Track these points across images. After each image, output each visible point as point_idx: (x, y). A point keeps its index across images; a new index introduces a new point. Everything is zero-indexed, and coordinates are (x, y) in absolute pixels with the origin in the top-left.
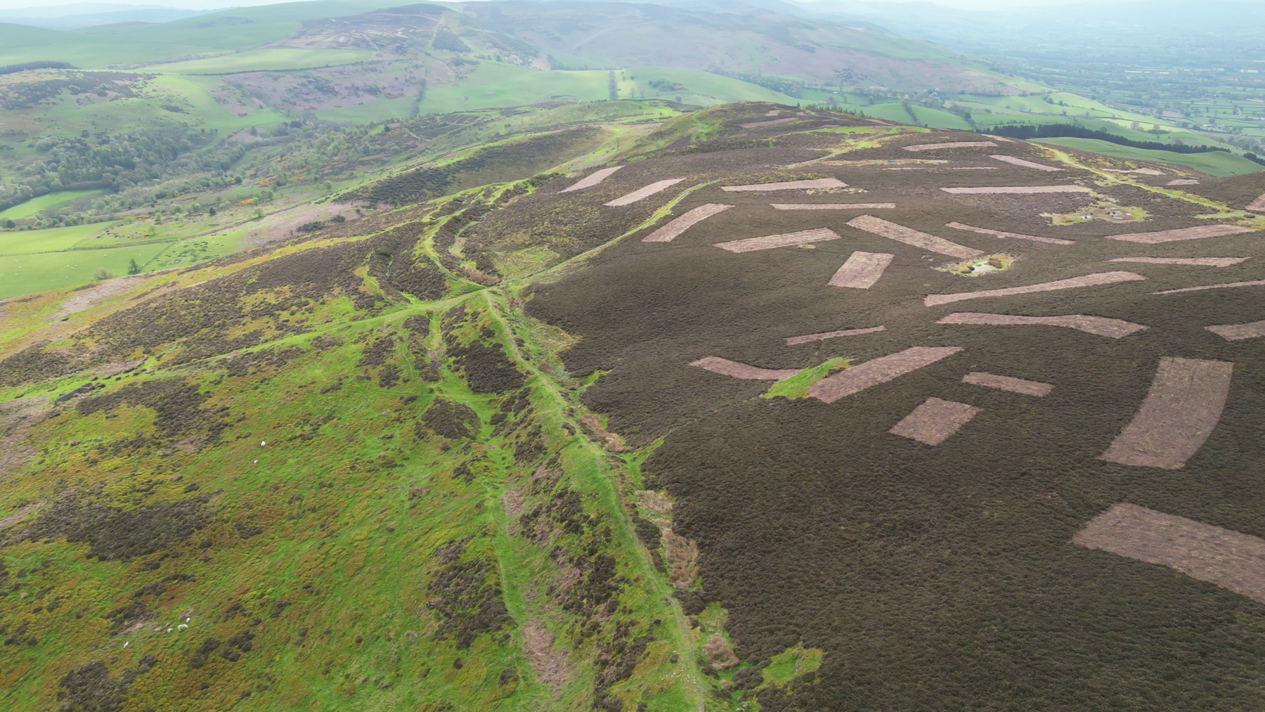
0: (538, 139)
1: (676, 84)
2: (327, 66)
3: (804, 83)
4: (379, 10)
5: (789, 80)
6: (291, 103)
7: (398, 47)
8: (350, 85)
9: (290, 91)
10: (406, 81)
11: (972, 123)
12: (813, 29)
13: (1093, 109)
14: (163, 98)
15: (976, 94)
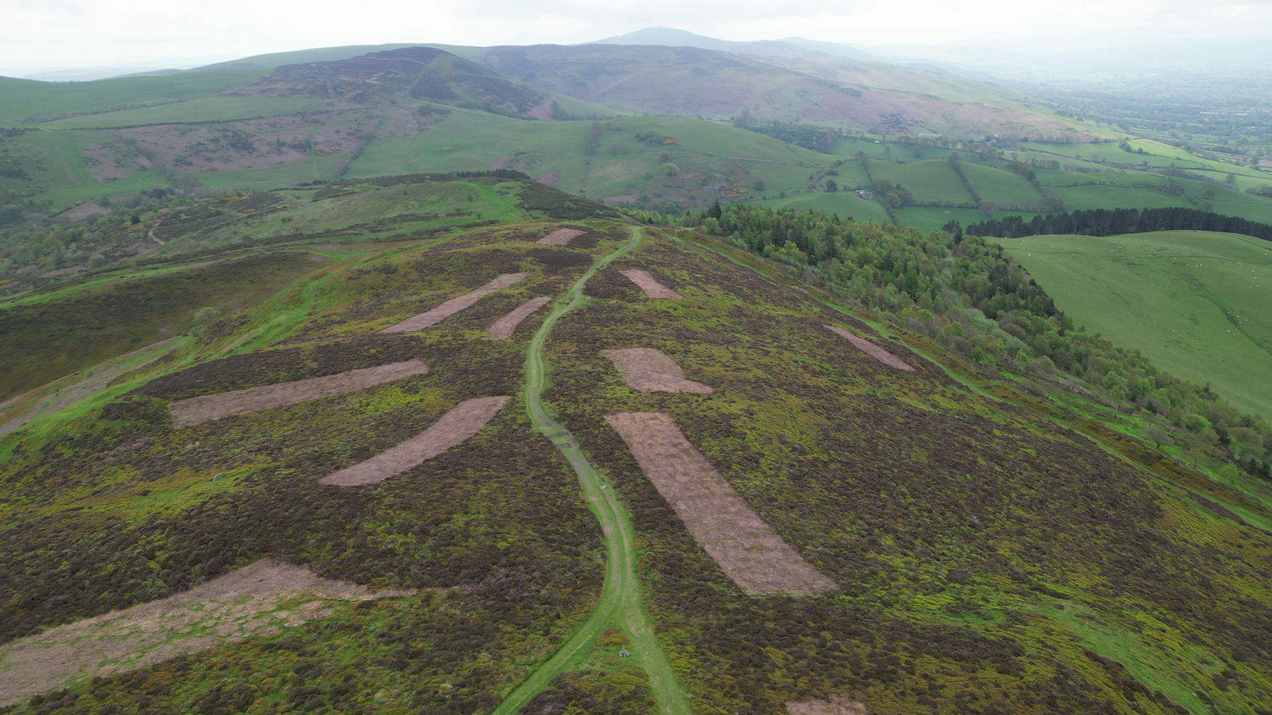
0: (137, 286)
1: (666, 138)
2: (260, 117)
3: (841, 132)
4: (368, 55)
5: (824, 128)
6: (186, 164)
7: (358, 95)
8: (274, 139)
9: (191, 147)
10: (349, 134)
11: (1037, 186)
12: (864, 71)
13: (1178, 158)
14: (9, 160)
15: (1042, 142)
